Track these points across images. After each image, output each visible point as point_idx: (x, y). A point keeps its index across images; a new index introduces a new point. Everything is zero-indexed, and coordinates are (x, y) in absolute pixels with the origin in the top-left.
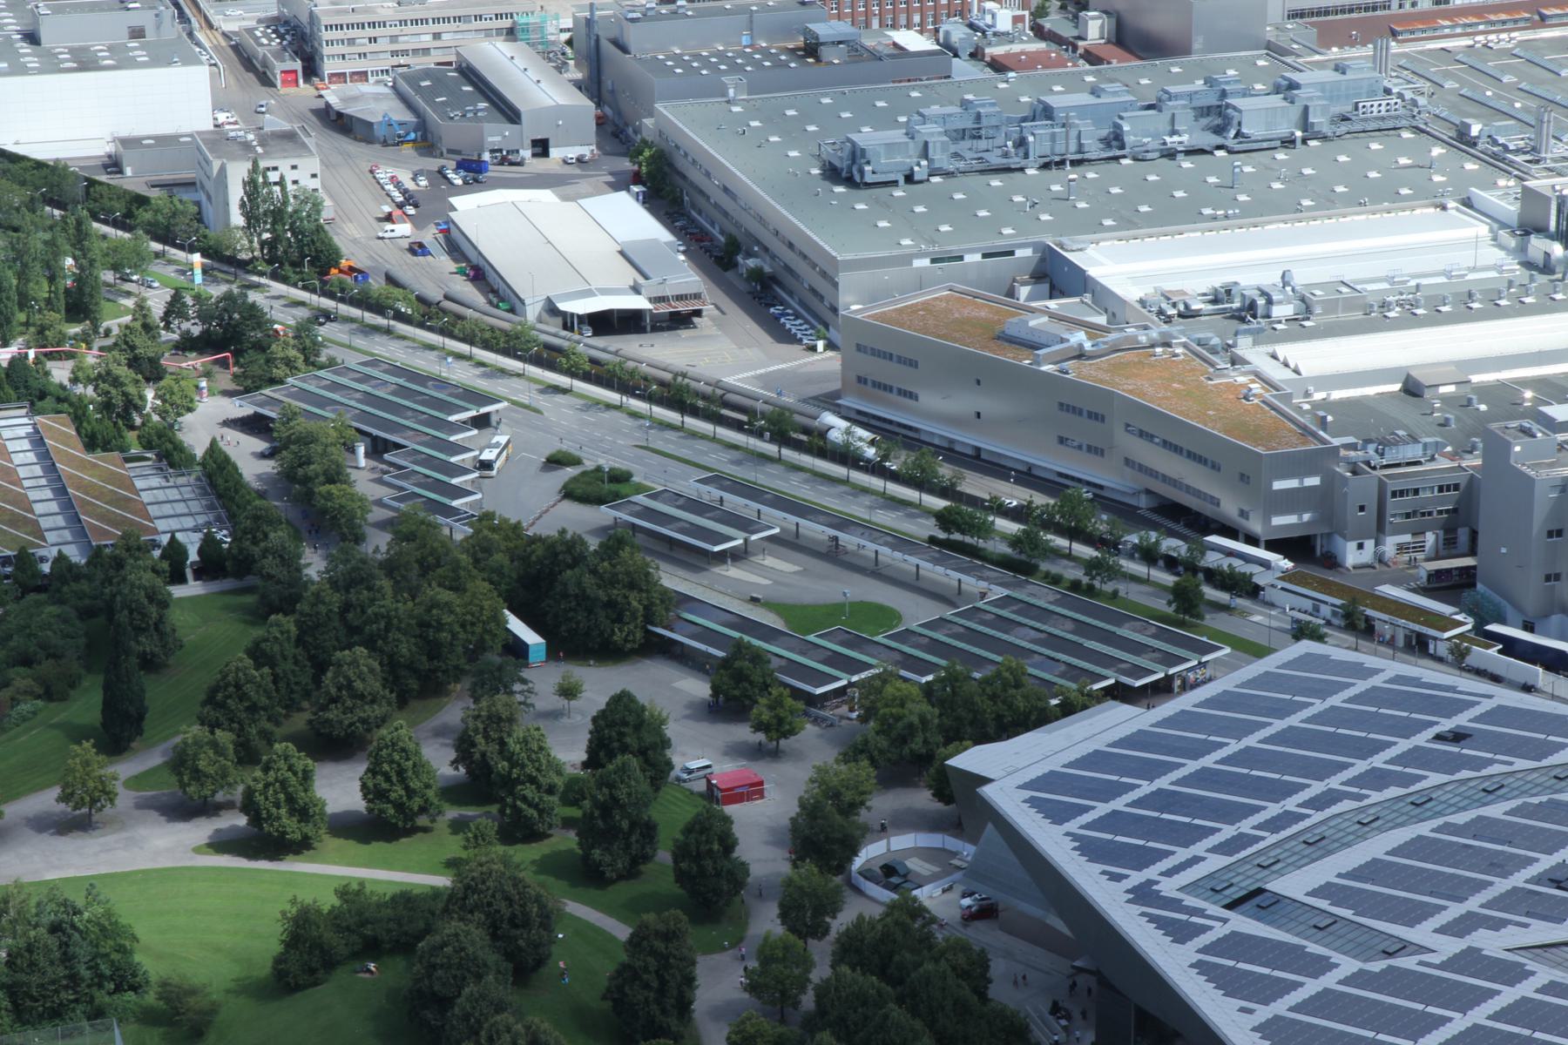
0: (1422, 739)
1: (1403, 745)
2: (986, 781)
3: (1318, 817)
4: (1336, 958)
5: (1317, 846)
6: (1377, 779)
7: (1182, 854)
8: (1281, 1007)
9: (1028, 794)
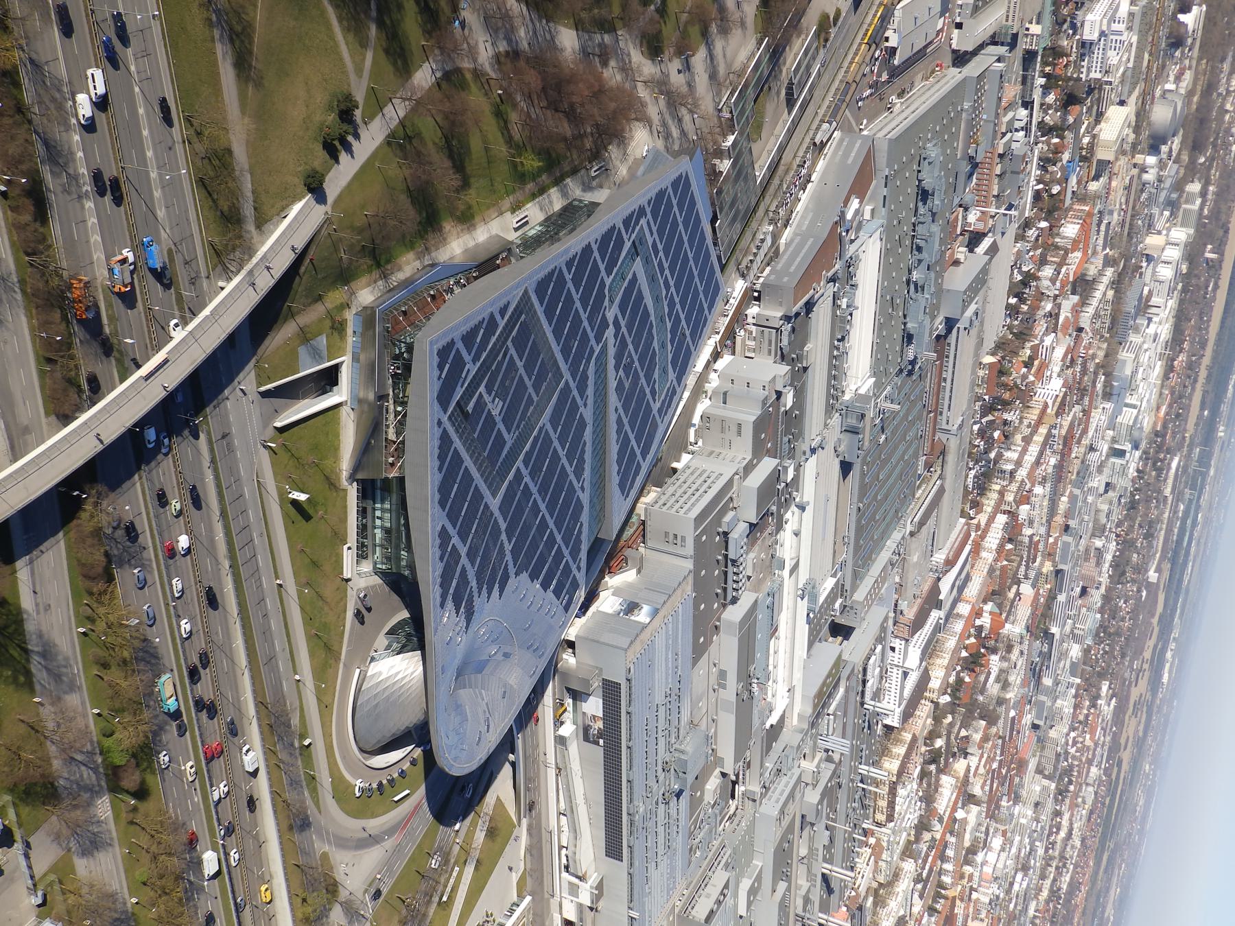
1: (682, 316)
4: (611, 277)
5: (652, 279)
7: (654, 229)
8: (596, 254)
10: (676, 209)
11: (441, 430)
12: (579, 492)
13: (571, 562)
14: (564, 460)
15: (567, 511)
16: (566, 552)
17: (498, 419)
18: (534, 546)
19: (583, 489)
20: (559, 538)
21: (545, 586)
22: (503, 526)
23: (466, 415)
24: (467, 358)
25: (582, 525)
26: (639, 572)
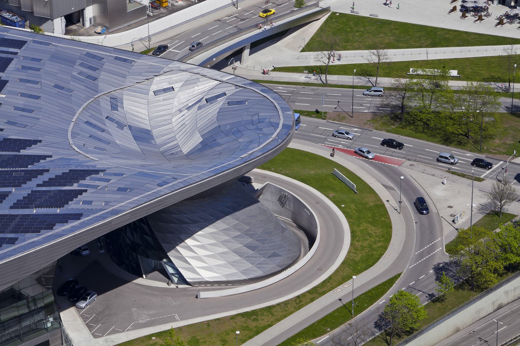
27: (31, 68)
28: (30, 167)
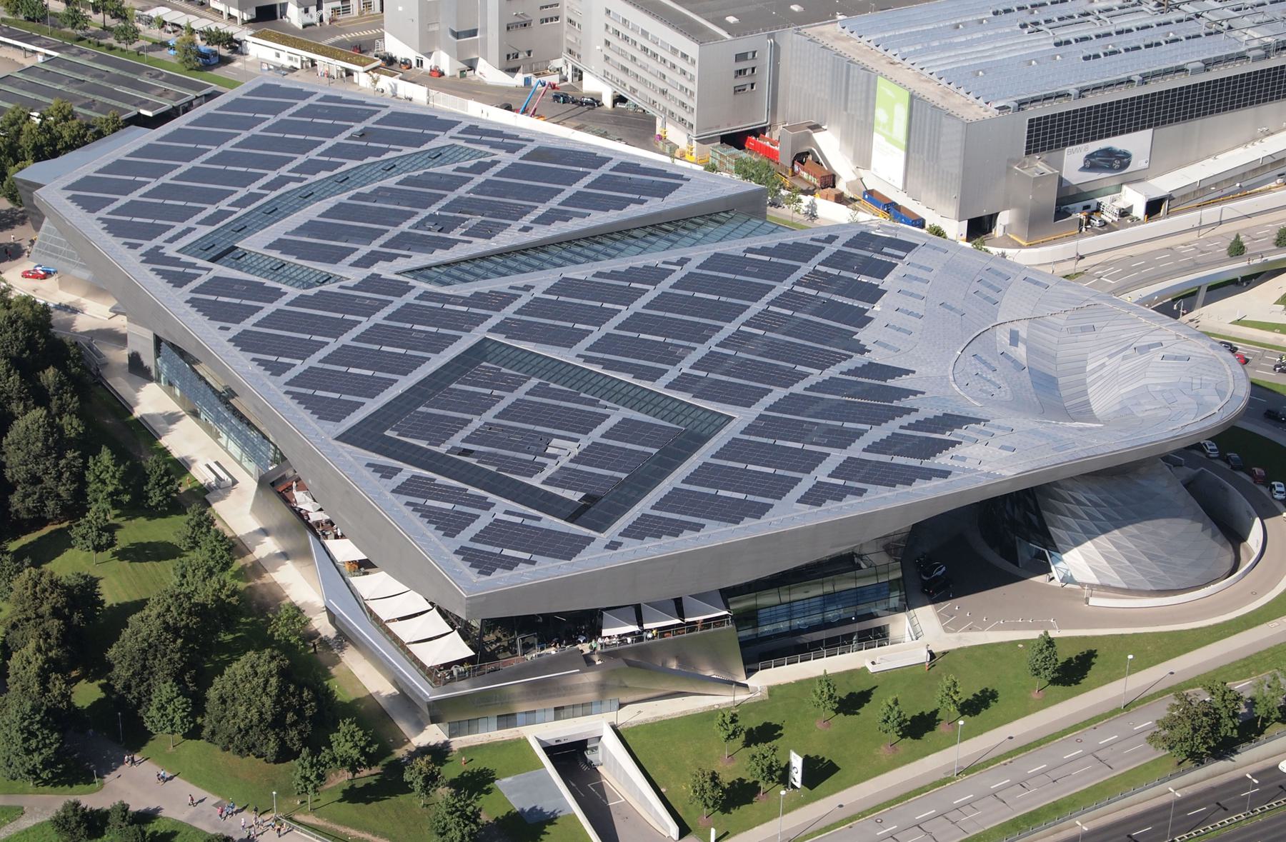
0: (341, 138)
1: (330, 143)
2: (40, 186)
3: (273, 194)
4: (284, 288)
5: (273, 213)
6: (312, 167)
7: (180, 227)
8: (248, 324)
9: (70, 193)
10: (135, 196)
11: (625, 540)
12: (691, 267)
13: (822, 256)
14: (638, 306)
15: (730, 282)
16: (805, 269)
17: (585, 441)
18: (803, 329)
19: (682, 262)
20: (782, 288)
21: (874, 294)
22: (778, 393)
23: (590, 499)
24: (484, 520)
25: (750, 250)
26: (816, 127)
27: (916, 279)
28: (895, 403)
